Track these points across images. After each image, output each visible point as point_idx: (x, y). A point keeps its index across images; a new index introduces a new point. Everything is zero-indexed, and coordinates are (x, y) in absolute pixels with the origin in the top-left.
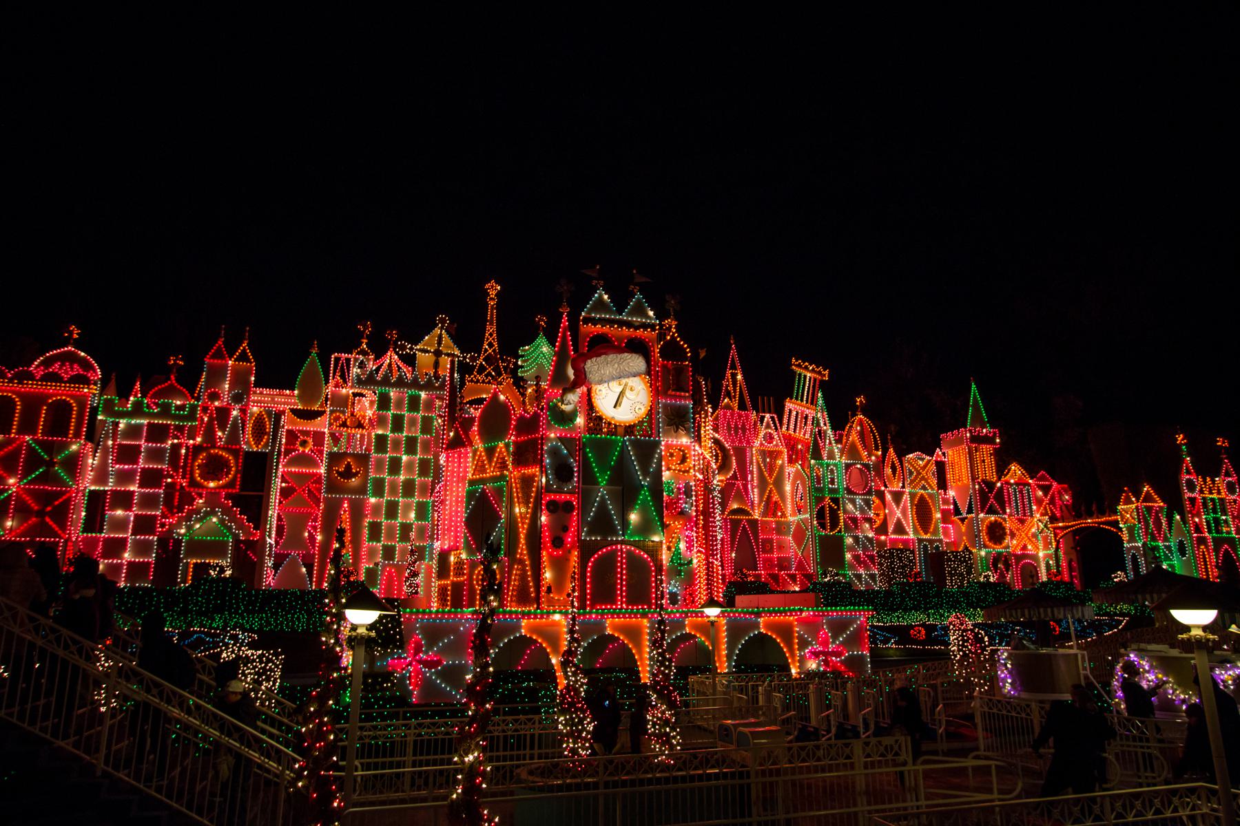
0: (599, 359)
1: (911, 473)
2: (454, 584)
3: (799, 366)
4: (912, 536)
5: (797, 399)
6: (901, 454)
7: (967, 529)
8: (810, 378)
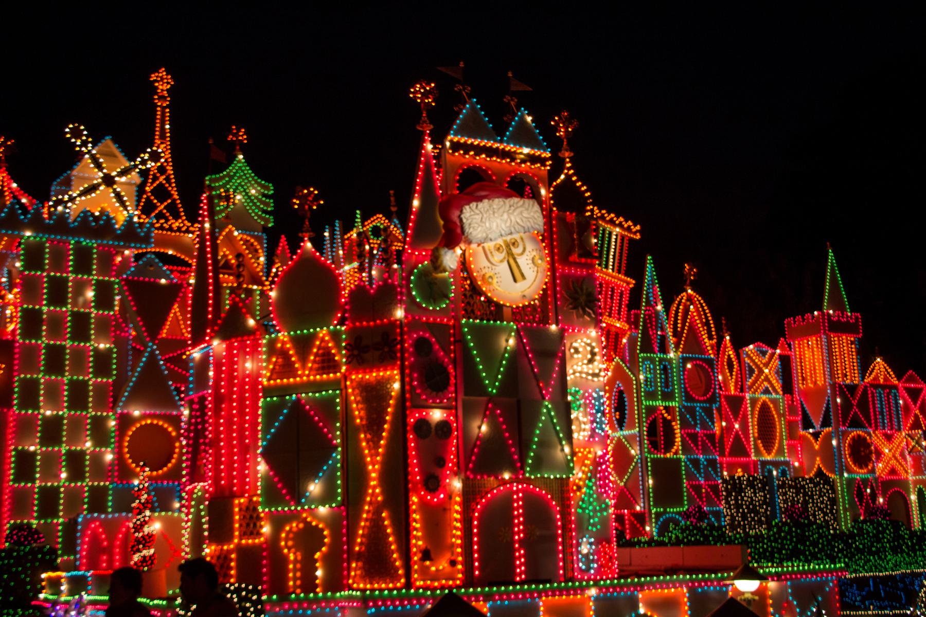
0: (480, 205)
1: (751, 371)
2: (240, 549)
4: (754, 458)
6: (738, 345)
7: (821, 446)
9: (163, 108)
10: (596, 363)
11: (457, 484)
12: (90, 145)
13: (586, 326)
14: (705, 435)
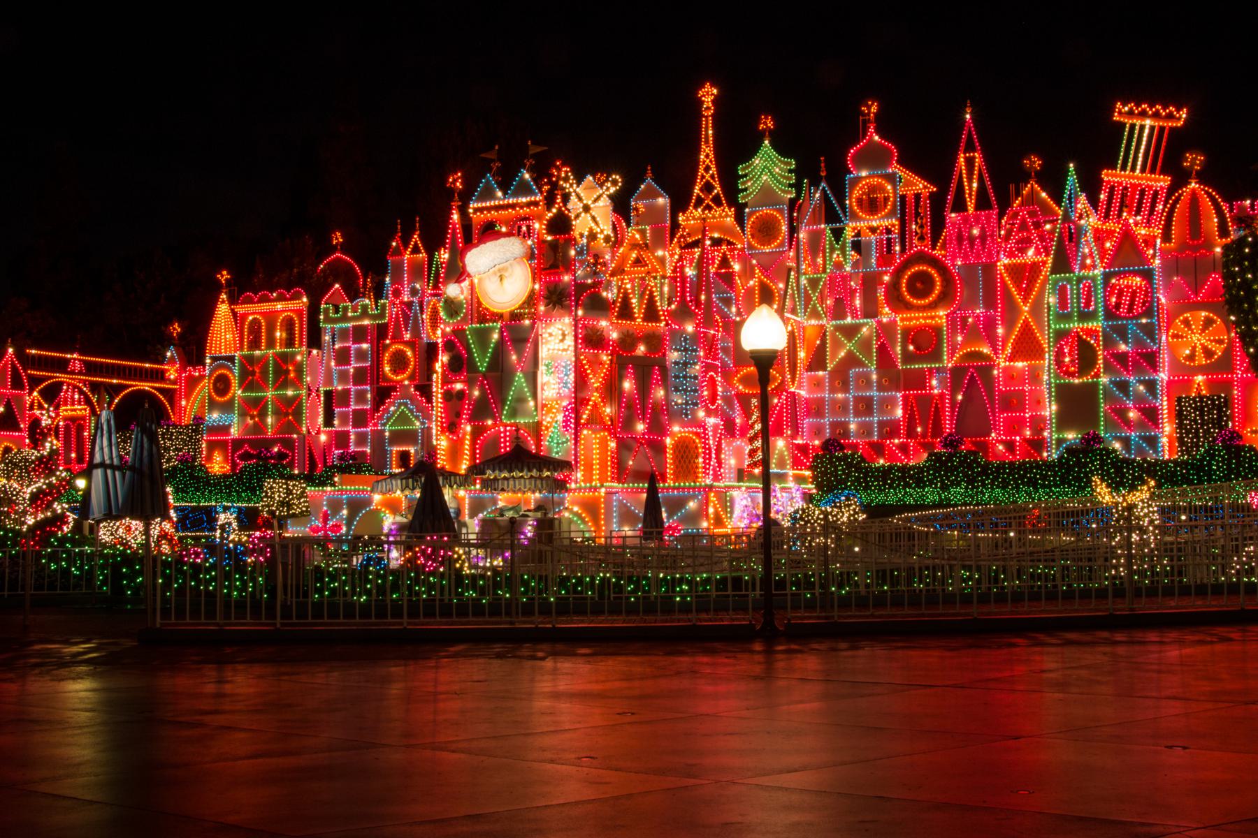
3: (1131, 113)
5: (1124, 168)
8: (1152, 128)
9: (707, 117)
10: (565, 342)
11: (469, 428)
12: (575, 186)
13: (561, 316)
14: (1138, 354)
